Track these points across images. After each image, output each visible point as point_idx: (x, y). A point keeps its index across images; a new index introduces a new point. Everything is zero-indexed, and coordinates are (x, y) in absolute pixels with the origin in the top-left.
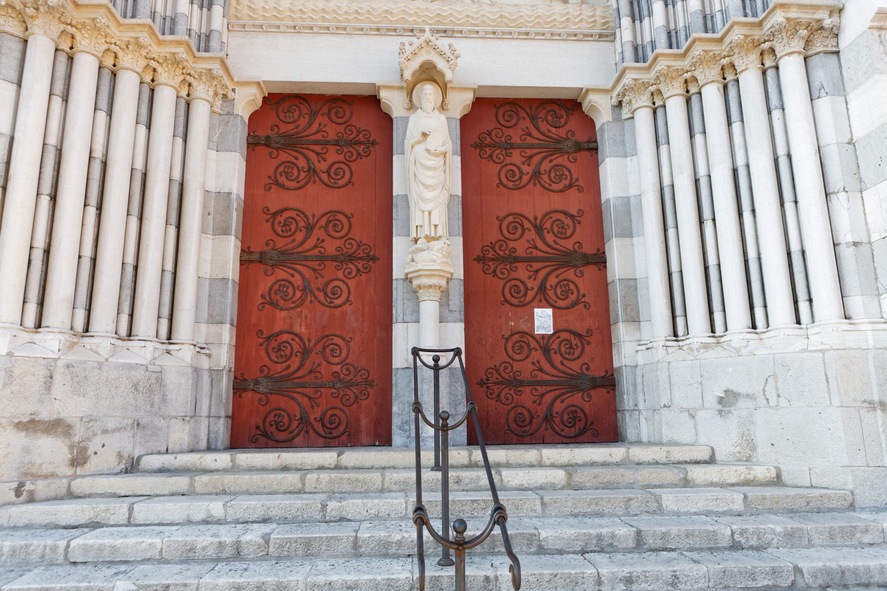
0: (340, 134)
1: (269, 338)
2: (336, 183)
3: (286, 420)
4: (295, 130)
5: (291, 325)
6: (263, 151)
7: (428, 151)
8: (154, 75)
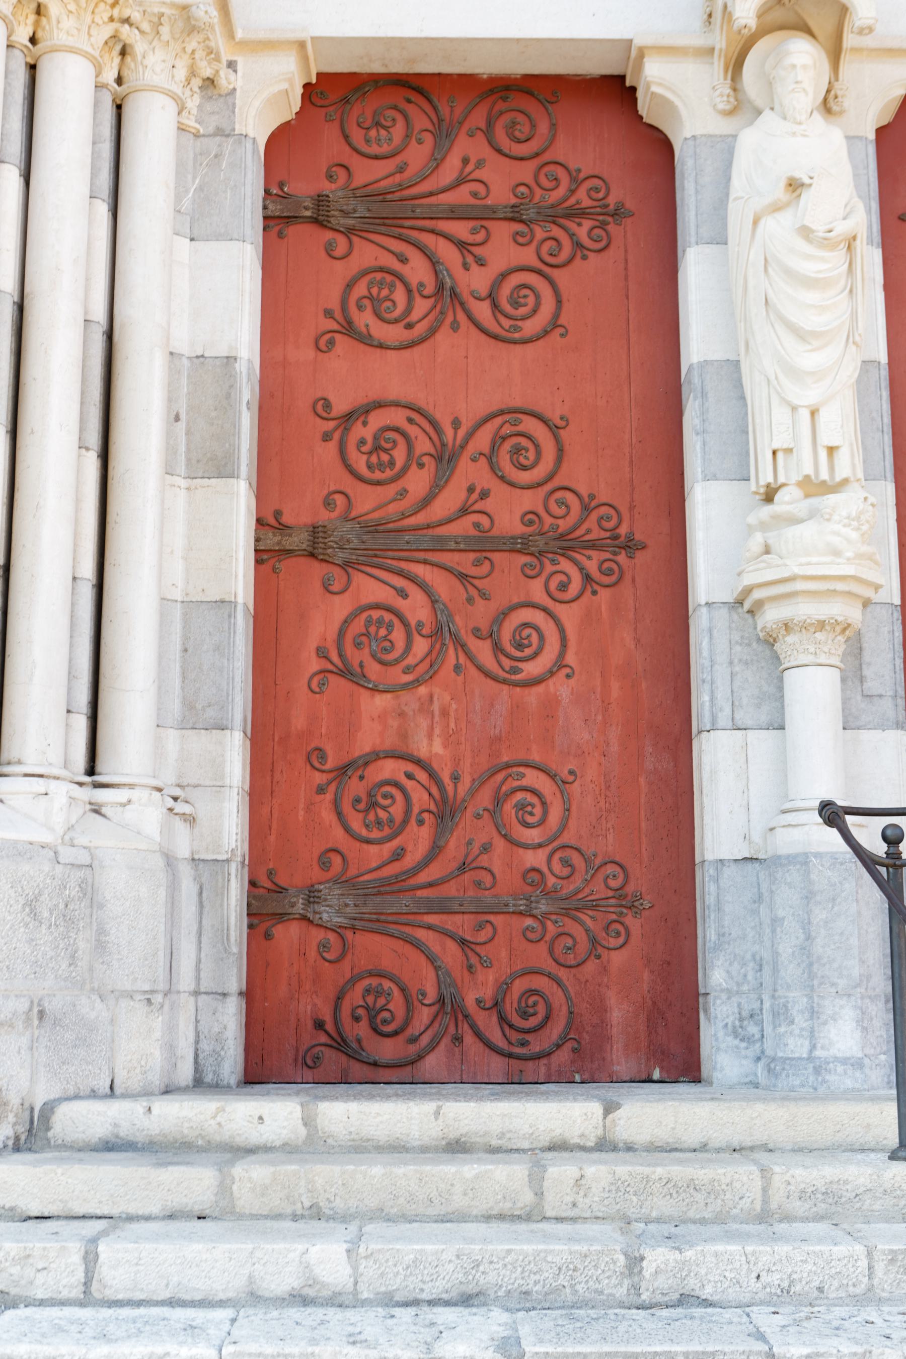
0: (522, 189)
1: (343, 771)
2: (517, 329)
3: (397, 1004)
4: (397, 178)
5: (404, 735)
7: (805, 232)
8: (37, 24)
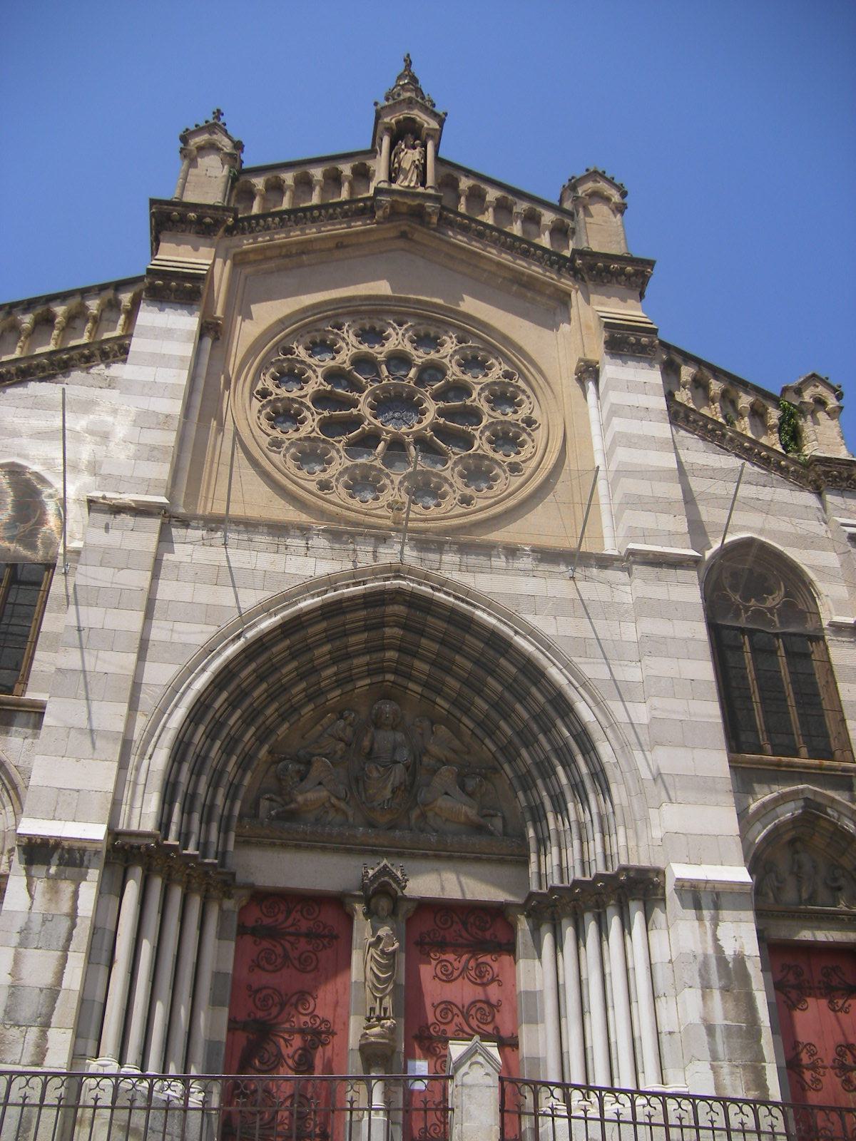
6: (248, 939)
